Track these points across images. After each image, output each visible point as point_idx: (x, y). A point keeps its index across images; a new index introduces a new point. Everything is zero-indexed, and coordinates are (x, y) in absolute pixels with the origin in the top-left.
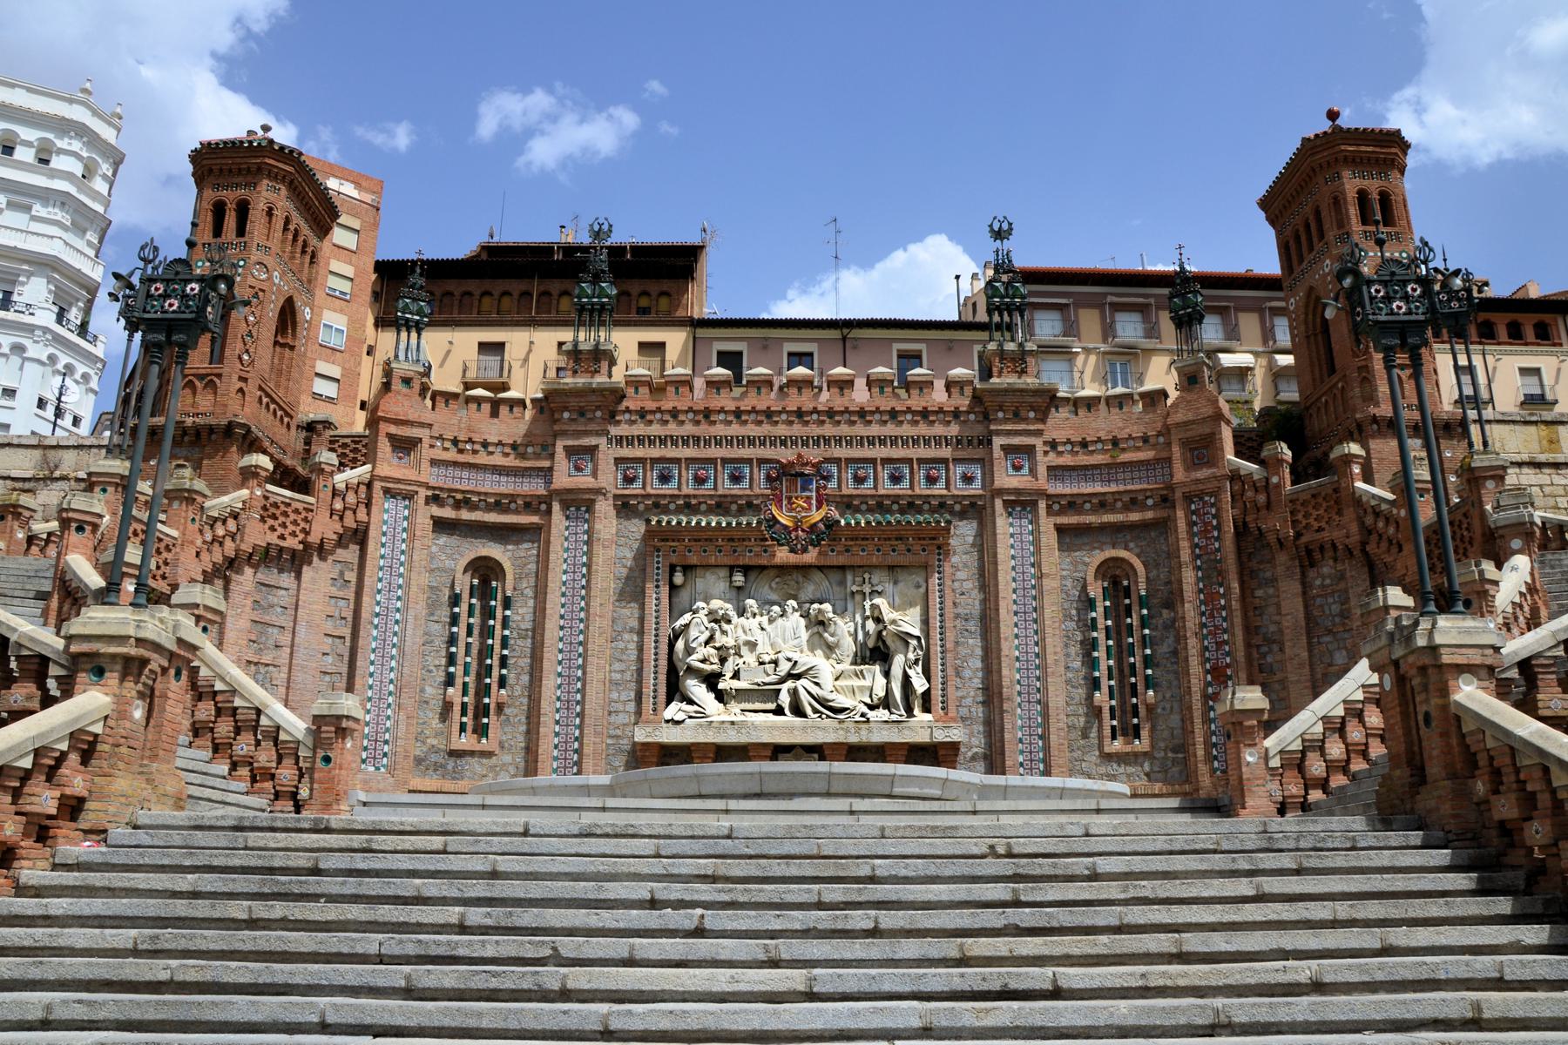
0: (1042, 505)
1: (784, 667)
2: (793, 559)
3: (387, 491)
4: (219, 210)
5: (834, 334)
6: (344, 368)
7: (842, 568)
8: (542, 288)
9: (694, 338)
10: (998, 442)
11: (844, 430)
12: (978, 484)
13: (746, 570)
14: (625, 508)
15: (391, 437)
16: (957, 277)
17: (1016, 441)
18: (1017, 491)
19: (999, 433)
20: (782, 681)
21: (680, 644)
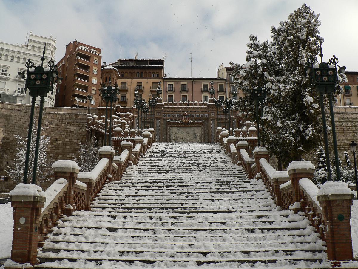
0: (215, 120)
1: (184, 139)
2: (185, 126)
3: (135, 118)
4: (106, 78)
5: (191, 81)
6: (96, 88)
7: (190, 127)
8: (134, 71)
9: (163, 81)
10: (210, 112)
11: (191, 110)
12: (208, 117)
13: (179, 127)
14: (164, 119)
15: (135, 111)
16: (217, 65)
17: (212, 111)
18: (212, 118)
19: (210, 110)
20: (183, 141)
21: (171, 136)
